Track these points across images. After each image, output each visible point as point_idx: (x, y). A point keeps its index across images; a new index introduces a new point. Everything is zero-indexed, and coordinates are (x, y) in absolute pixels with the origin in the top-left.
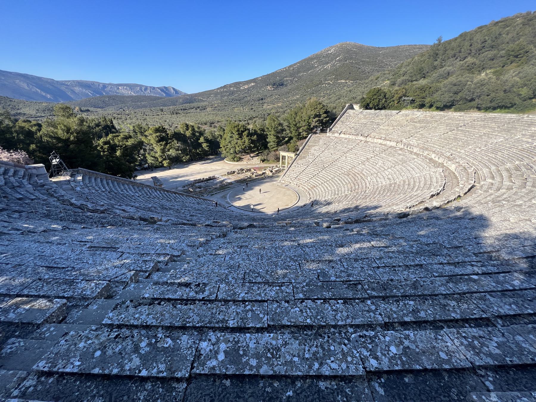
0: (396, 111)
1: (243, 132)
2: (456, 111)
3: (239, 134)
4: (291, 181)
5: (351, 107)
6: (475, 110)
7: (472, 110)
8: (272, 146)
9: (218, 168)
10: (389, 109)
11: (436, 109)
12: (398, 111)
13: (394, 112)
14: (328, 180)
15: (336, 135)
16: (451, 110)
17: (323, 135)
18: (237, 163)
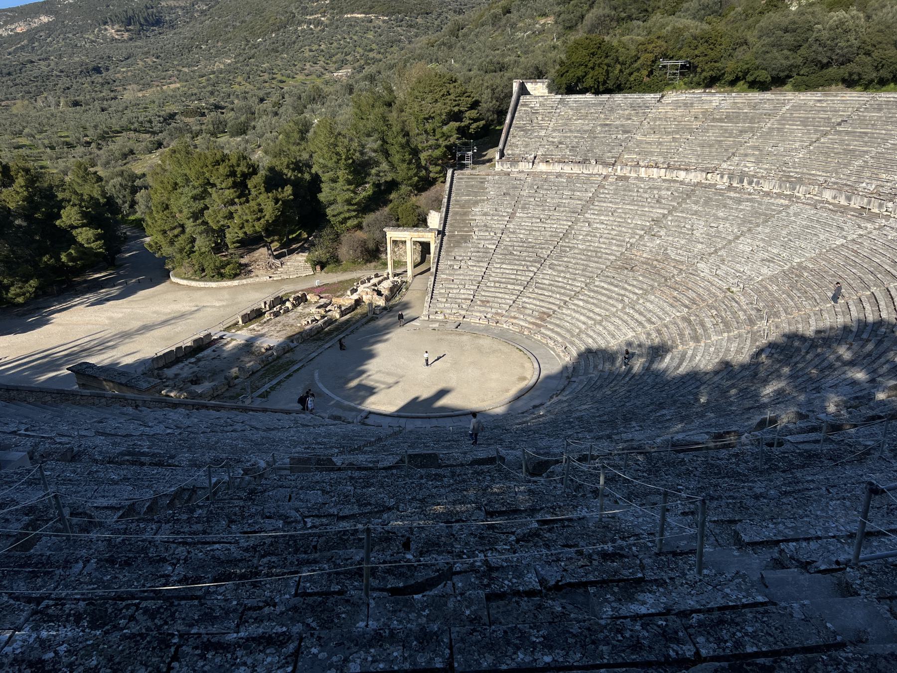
0: (652, 95)
1: (246, 176)
2: (797, 88)
3: (235, 185)
4: (463, 313)
5: (523, 91)
6: (840, 86)
7: (833, 87)
8: (340, 218)
9: (184, 306)
10: (631, 89)
11: (750, 87)
12: (658, 96)
13: (650, 97)
14: (578, 289)
15: (524, 166)
16: (785, 87)
17: (481, 170)
18: (236, 283)
